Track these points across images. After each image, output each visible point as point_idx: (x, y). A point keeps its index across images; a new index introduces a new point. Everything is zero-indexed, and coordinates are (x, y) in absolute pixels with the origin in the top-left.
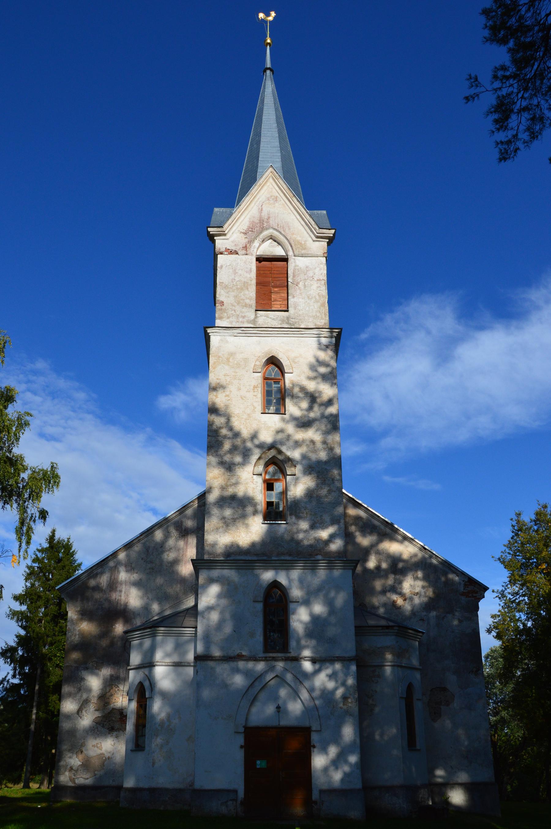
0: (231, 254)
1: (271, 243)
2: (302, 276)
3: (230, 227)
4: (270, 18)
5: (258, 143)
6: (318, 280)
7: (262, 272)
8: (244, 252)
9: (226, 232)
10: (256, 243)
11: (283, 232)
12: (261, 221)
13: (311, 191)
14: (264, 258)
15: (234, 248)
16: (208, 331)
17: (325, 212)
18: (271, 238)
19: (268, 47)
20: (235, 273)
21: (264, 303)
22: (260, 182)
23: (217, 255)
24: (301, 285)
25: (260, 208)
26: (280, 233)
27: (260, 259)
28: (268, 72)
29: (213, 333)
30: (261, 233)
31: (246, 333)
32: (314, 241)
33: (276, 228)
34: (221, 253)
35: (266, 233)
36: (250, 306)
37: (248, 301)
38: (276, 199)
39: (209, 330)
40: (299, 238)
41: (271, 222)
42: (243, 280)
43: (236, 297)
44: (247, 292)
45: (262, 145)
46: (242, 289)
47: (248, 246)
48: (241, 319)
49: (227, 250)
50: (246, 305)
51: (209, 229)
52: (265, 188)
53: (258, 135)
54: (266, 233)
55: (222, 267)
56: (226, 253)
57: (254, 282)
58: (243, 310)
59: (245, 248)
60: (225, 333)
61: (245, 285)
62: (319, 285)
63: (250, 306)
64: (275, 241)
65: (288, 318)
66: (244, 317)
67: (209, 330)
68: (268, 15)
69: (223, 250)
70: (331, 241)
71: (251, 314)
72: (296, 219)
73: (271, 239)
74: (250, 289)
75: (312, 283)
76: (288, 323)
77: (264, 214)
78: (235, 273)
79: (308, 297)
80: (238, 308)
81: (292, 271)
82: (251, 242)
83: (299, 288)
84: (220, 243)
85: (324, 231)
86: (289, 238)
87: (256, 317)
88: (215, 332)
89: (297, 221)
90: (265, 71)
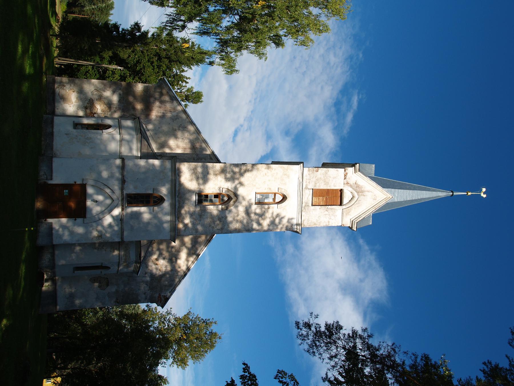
4: (482, 195)
5: (410, 189)
8: (345, 183)
10: (351, 189)
12: (362, 192)
13: (383, 217)
15: (347, 177)
17: (371, 223)
18: (353, 197)
20: (334, 178)
21: (317, 193)
22: (384, 191)
24: (326, 213)
27: (341, 191)
28: (451, 193)
35: (356, 194)
36: (315, 186)
37: (318, 185)
38: (375, 199)
39: (302, 165)
41: (362, 197)
43: (321, 178)
44: (323, 184)
45: (408, 191)
48: (308, 181)
49: (347, 174)
50: (316, 184)
51: (358, 165)
53: (414, 189)
54: (356, 194)
57: (329, 188)
61: (327, 183)
63: (315, 186)
65: (308, 206)
66: (309, 183)
68: (484, 193)
69: (347, 171)
70: (351, 228)
71: (311, 186)
76: (305, 206)
77: (366, 193)
78: (334, 178)
80: (314, 179)
82: (351, 186)
84: (350, 170)
87: (309, 189)
90: (452, 192)
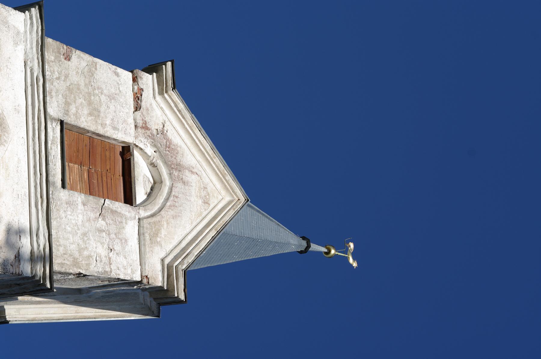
0: (135, 99)
1: (149, 181)
2: (113, 228)
3: (173, 105)
4: (351, 260)
6: (110, 258)
7: (107, 153)
8: (140, 123)
9: (166, 95)
11: (168, 204)
14: (129, 161)
15: (143, 104)
16: (33, 10)
19: (326, 251)
23: (132, 72)
24: (101, 223)
25: (194, 170)
26: (167, 199)
27: (126, 152)
28: (304, 243)
29: (31, 18)
30: (165, 163)
31: (32, 85)
32: (163, 260)
33: (173, 193)
34: (135, 80)
39: (35, 11)
40: (163, 232)
42: (102, 109)
44: (86, 112)
46: (90, 103)
47: (148, 132)
50: (67, 104)
52: (219, 186)
55: (117, 75)
56: (136, 87)
58: (60, 96)
59: (145, 127)
60: (32, 44)
61: (95, 112)
62: (104, 259)
63: (67, 112)
64: (152, 189)
67: (35, 11)
72: (186, 232)
73: (155, 183)
74: (90, 118)
75: (106, 246)
79: (85, 234)
81: (119, 210)
83: (96, 219)
84: (148, 80)
85: (181, 280)
86: (162, 212)
88: (32, 23)
89: (183, 235)
